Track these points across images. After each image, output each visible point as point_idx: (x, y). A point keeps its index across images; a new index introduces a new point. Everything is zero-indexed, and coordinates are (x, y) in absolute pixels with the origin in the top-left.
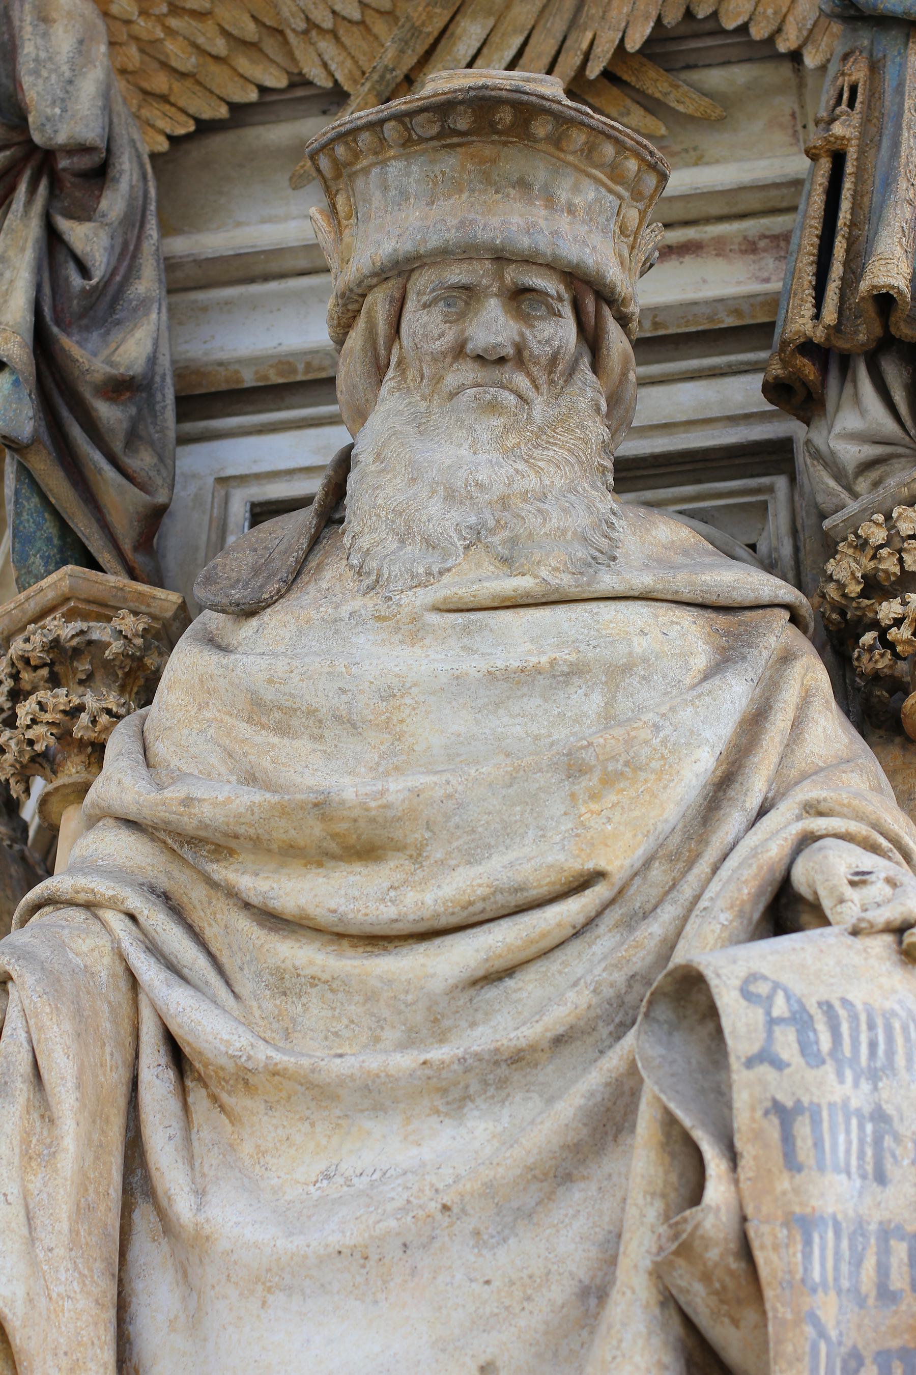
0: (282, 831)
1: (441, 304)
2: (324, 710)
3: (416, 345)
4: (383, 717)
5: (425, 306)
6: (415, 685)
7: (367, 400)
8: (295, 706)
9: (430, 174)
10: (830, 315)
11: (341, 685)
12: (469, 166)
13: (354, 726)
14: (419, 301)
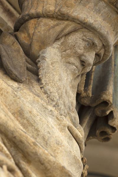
0: (57, 174)
1: (87, 43)
2: (41, 133)
3: (74, 45)
4: (55, 148)
5: (83, 40)
6: (63, 146)
7: (50, 43)
8: (33, 124)
9: (108, 13)
10: (90, 93)
11: (49, 131)
12: (115, 20)
13: (47, 144)
14: (83, 37)
